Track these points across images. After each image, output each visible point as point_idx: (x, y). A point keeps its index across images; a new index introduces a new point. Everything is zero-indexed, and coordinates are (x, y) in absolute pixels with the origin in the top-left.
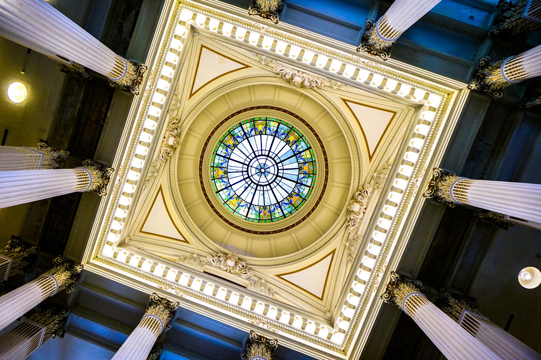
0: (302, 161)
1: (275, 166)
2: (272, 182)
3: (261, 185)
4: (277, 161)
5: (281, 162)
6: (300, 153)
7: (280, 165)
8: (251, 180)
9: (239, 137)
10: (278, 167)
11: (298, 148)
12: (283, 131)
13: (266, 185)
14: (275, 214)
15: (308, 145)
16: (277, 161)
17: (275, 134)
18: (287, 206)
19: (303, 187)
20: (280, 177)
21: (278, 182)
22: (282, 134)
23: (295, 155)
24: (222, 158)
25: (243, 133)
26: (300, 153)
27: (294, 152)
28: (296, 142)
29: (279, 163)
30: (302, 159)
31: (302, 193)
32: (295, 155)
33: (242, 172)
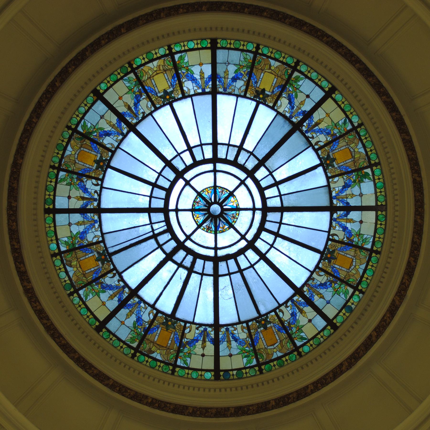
0: (323, 139)
1: (249, 182)
2: (257, 236)
3: (226, 258)
4: (250, 165)
5: (262, 163)
6: (308, 115)
7: (261, 174)
8: (189, 251)
9: (108, 134)
10: (257, 182)
11: (297, 102)
12: (232, 69)
13: (242, 252)
14: (300, 329)
15: (325, 84)
16: (250, 165)
17: (214, 86)
18: (328, 293)
19: (354, 215)
20: (274, 209)
21: (273, 227)
22: (234, 79)
23: (296, 127)
24: (77, 217)
25: (114, 119)
26: (308, 115)
27: (288, 119)
28: (283, 88)
29: (256, 168)
30: (321, 131)
31: (359, 235)
32: (296, 127)
33: (155, 236)
